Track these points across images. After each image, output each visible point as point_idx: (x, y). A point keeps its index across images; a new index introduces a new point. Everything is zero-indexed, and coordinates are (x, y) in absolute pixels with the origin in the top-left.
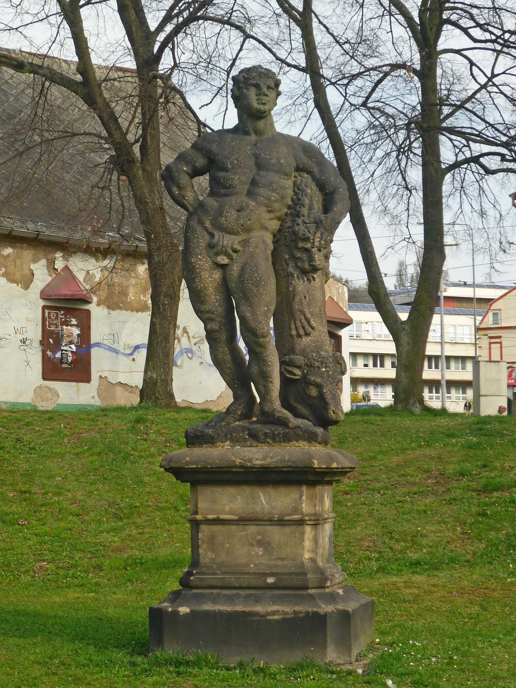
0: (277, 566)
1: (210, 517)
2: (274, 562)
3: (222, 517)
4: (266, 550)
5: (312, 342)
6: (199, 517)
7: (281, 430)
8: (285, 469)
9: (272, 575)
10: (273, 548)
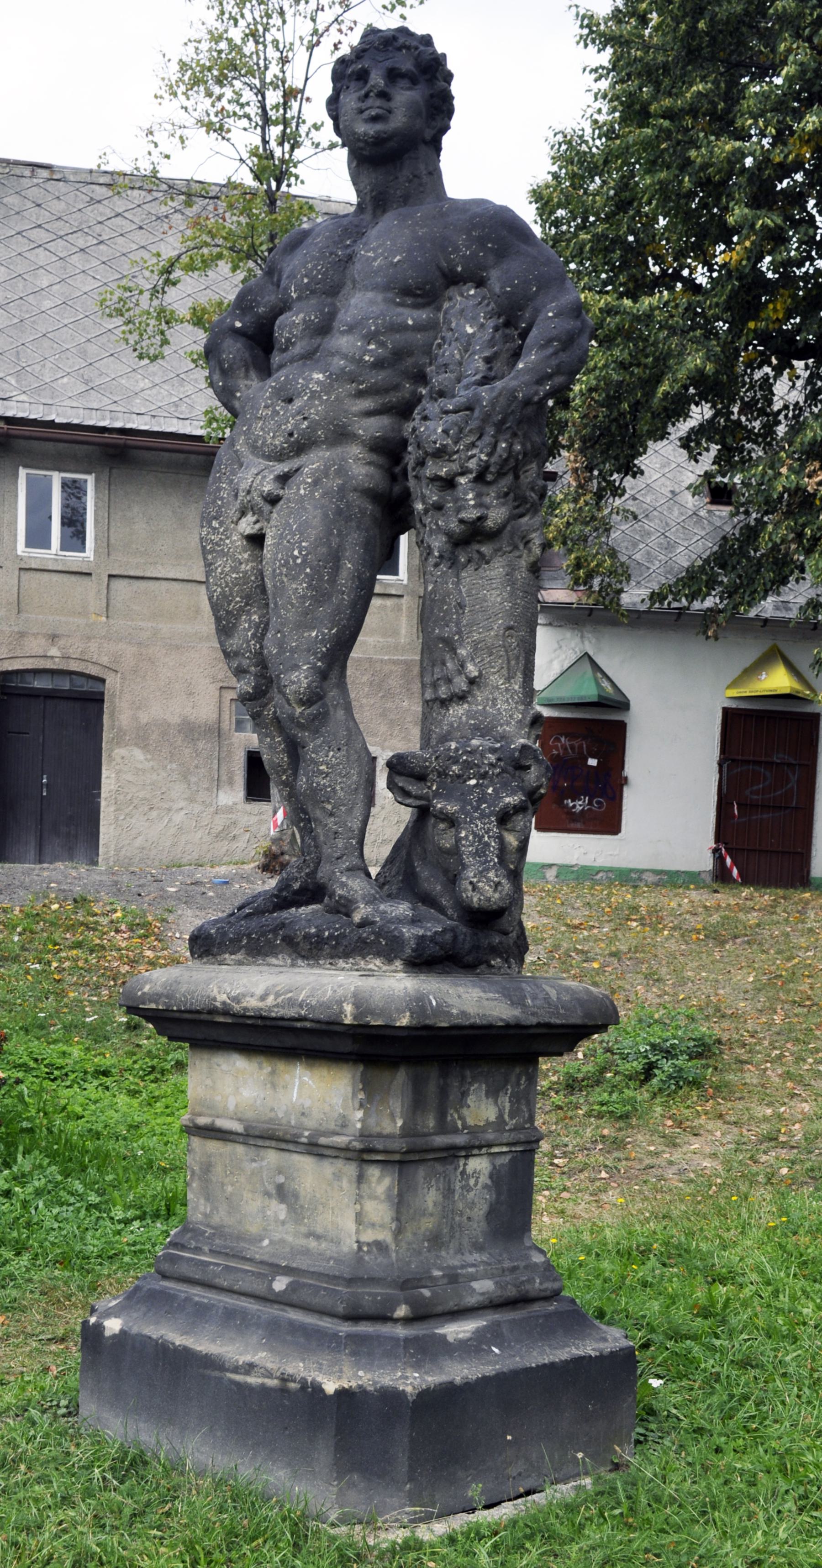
0: (306, 1252)
2: (303, 1242)
3: (222, 1123)
4: (291, 1209)
5: (469, 717)
8: (299, 1025)
9: (287, 1271)
10: (302, 1207)
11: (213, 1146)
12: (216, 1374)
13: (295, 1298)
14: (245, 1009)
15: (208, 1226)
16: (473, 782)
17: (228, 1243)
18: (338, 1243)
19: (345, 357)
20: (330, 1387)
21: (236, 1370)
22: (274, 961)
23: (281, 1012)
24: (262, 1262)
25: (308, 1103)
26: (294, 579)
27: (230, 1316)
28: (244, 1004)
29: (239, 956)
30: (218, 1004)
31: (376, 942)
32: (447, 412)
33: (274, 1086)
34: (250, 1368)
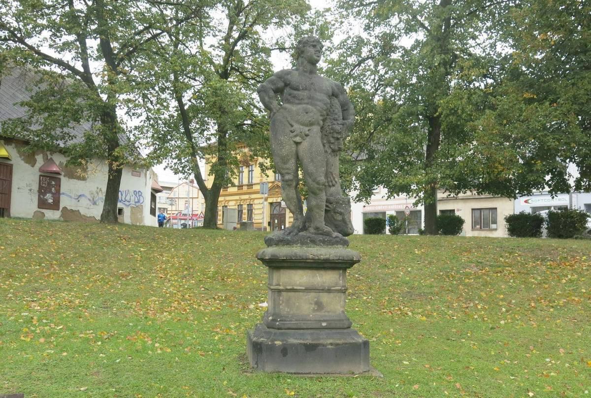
1: (289, 287)
3: (295, 288)
6: (281, 288)
9: (324, 321)
11: (292, 294)
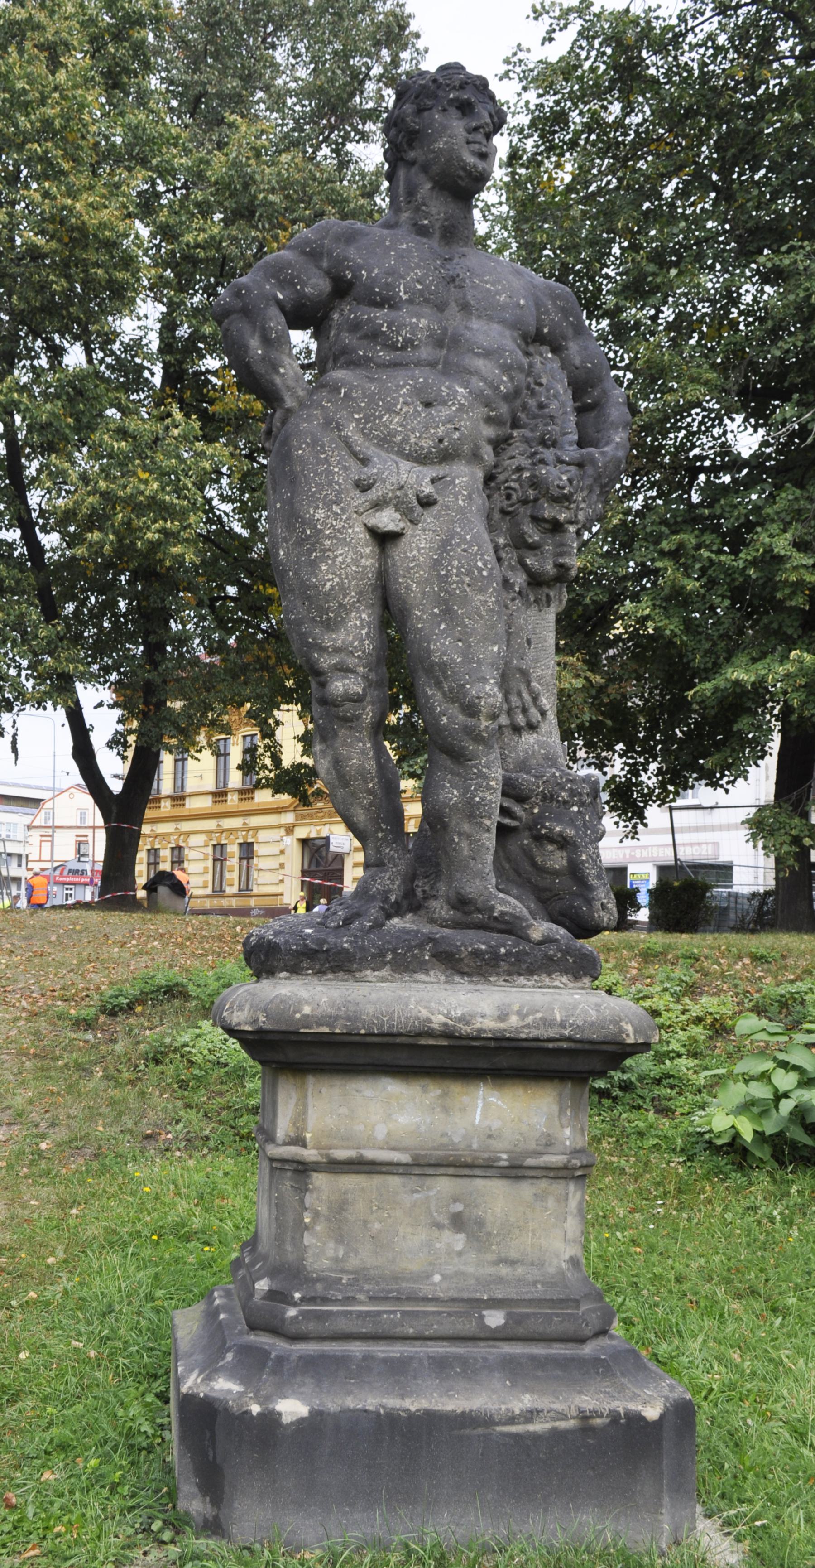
0: (500, 1280)
1: (341, 1154)
2: (491, 1270)
3: (371, 1154)
4: (473, 1238)
5: (540, 747)
6: (310, 1154)
7: (506, 946)
8: (551, 1045)
9: (495, 1303)
10: (489, 1234)
11: (350, 1182)
12: (480, 1431)
13: (520, 1331)
14: (479, 1030)
15: (342, 1271)
16: (575, 809)
17: (383, 1285)
18: (542, 1265)
19: (484, 379)
20: (652, 1413)
21: (512, 1420)
22: (423, 977)
23: (534, 1033)
24: (453, 1300)
25: (496, 1125)
26: (481, 590)
27: (441, 1365)
28: (478, 1025)
29: (385, 972)
30: (436, 1027)
31: (563, 959)
32: (562, 462)
33: (446, 1110)
34: (530, 1415)
